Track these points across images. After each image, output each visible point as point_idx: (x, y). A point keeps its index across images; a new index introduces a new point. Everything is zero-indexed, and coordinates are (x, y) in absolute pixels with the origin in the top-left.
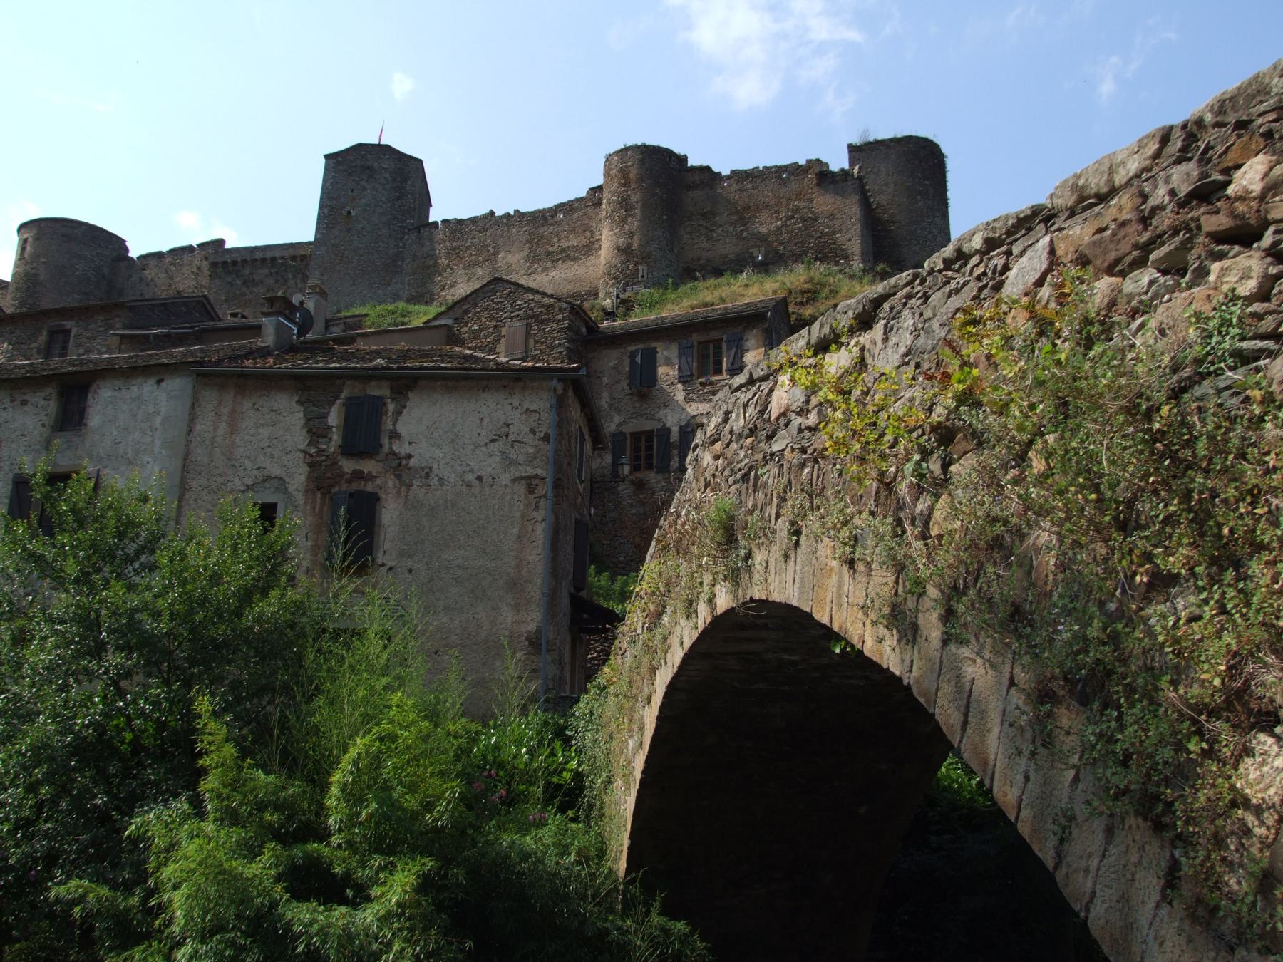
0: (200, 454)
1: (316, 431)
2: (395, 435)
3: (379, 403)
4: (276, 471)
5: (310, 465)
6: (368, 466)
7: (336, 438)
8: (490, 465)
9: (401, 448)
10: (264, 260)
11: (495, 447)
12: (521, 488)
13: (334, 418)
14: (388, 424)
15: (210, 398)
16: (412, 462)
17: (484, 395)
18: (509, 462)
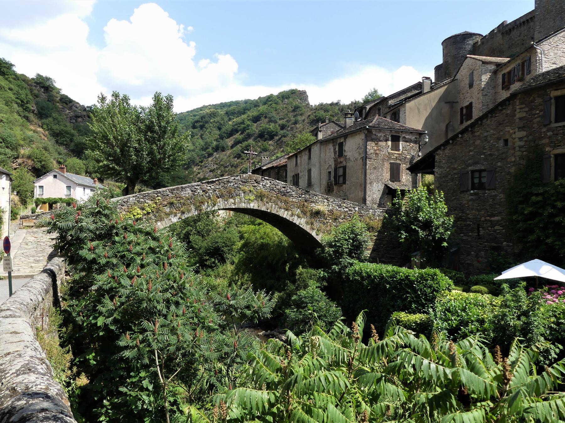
0: (322, 163)
1: (335, 153)
2: (345, 151)
3: (342, 143)
4: (331, 164)
5: (334, 161)
6: (342, 159)
7: (338, 153)
8: (357, 155)
9: (346, 154)
10: (520, 24)
11: (358, 150)
12: (361, 160)
13: (337, 149)
14: (344, 149)
15: (322, 147)
16: (347, 157)
17: (356, 137)
18: (360, 154)
